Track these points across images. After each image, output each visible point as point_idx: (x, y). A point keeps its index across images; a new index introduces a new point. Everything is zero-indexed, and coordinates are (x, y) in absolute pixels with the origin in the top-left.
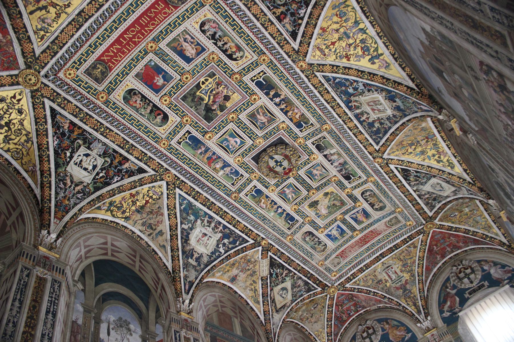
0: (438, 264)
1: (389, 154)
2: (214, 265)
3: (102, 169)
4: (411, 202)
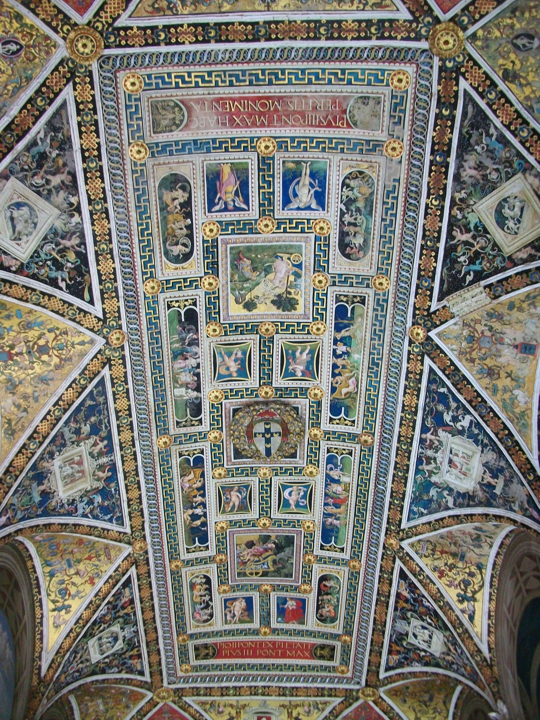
2: (496, 434)
3: (423, 620)
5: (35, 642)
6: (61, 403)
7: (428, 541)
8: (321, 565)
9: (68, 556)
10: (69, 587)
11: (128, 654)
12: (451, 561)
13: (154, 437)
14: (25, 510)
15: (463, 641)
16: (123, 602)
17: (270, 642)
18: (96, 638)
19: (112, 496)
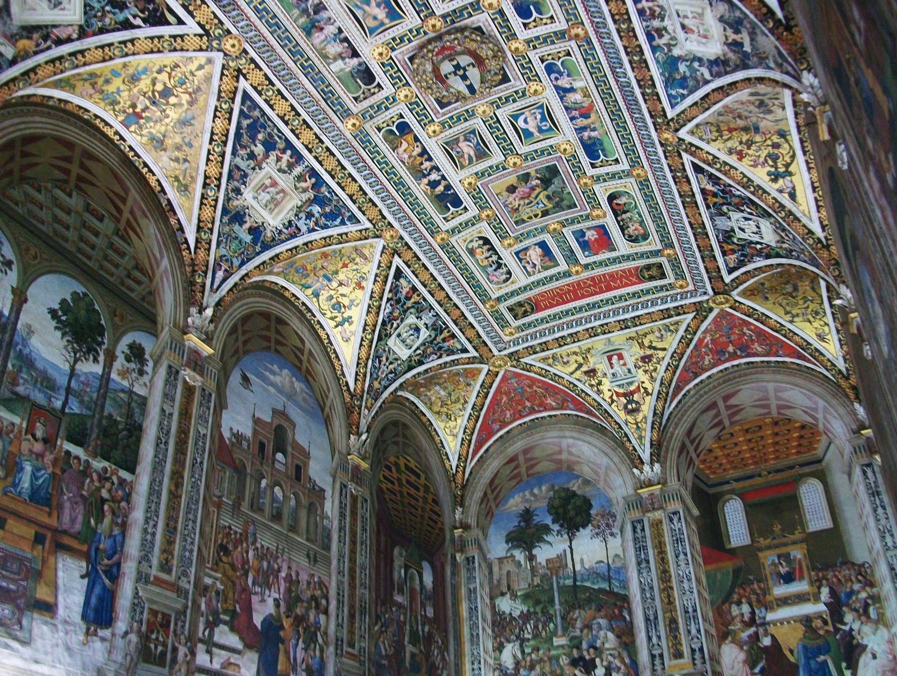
3: (742, 211)
5: (332, 362)
6: (215, 137)
7: (707, 123)
8: (603, 185)
9: (322, 273)
10: (340, 300)
11: (439, 339)
12: (745, 138)
13: (339, 124)
14: (240, 255)
15: (789, 225)
16: (404, 293)
17: (587, 279)
18: (394, 337)
19: (330, 200)
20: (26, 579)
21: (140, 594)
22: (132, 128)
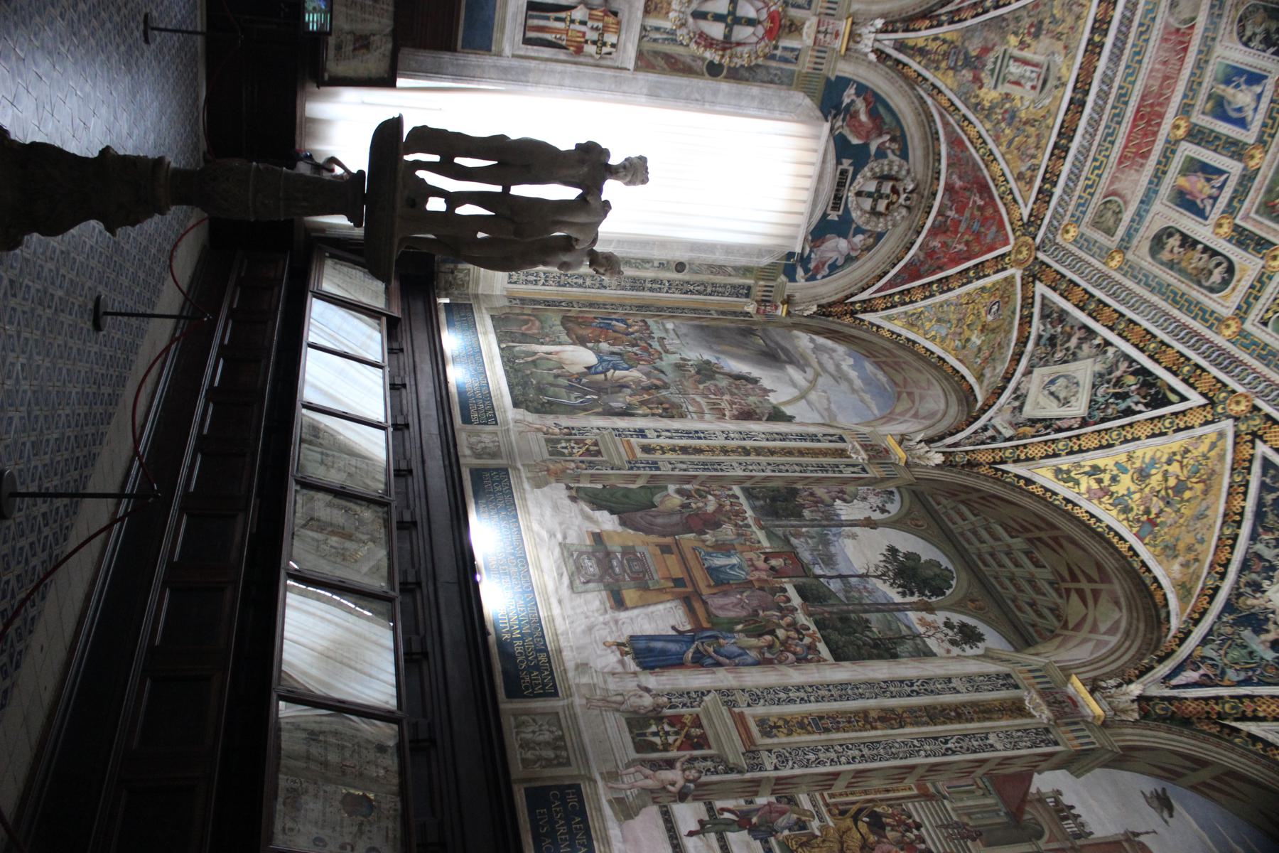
0: (949, 166)
1: (1221, 435)
4: (1100, 301)
20: (633, 579)
21: (705, 698)
22: (1147, 541)
